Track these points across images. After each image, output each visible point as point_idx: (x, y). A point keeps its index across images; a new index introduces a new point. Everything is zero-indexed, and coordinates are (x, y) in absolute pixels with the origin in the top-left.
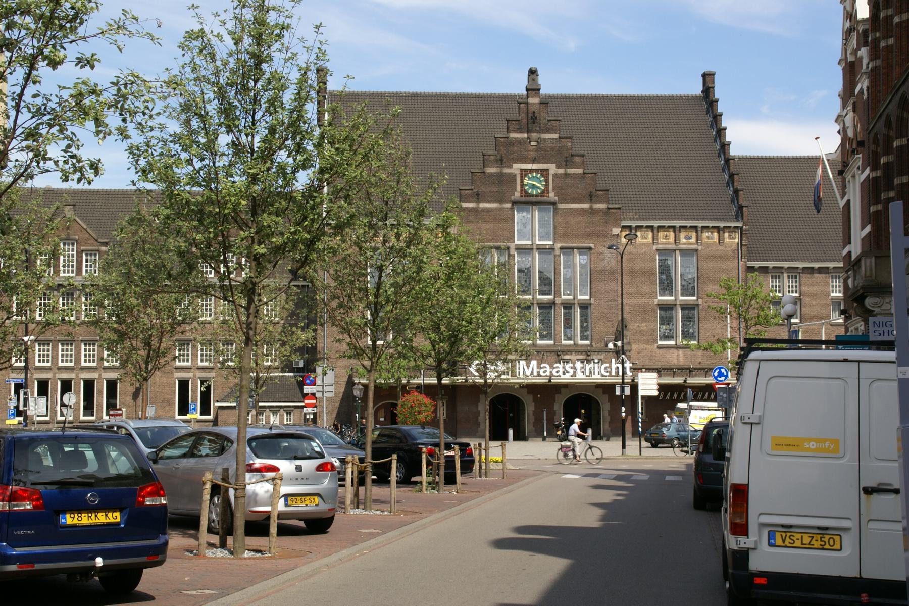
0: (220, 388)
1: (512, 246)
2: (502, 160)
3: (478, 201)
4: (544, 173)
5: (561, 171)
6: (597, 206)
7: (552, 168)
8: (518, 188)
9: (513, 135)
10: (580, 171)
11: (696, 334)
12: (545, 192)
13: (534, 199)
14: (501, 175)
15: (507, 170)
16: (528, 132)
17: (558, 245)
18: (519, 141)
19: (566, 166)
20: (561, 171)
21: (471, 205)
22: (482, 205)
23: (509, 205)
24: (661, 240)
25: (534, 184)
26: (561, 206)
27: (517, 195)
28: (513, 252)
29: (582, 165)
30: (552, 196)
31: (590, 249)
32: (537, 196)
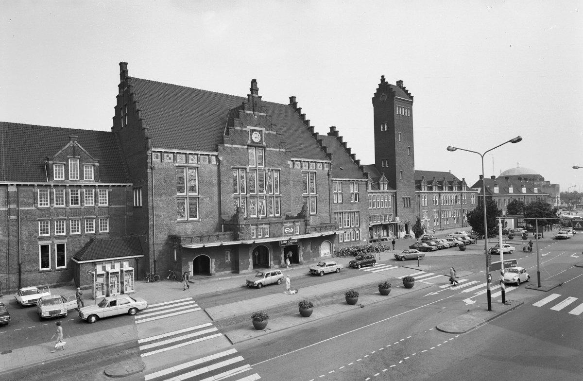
0: (71, 249)
1: (248, 168)
2: (242, 124)
3: (232, 144)
4: (260, 132)
5: (267, 132)
6: (282, 150)
7: (263, 129)
8: (250, 139)
9: (247, 112)
10: (275, 133)
11: (315, 209)
12: (261, 141)
13: (256, 145)
14: (242, 131)
15: (244, 129)
16: (253, 111)
17: (267, 168)
18: (250, 115)
19: (269, 130)
20: (267, 132)
21: (229, 146)
22: (234, 146)
23: (246, 147)
24: (303, 167)
25: (256, 138)
26: (268, 149)
27: (249, 142)
28: (248, 171)
29: (276, 130)
30: (264, 143)
31: (279, 170)
32: (257, 143)
